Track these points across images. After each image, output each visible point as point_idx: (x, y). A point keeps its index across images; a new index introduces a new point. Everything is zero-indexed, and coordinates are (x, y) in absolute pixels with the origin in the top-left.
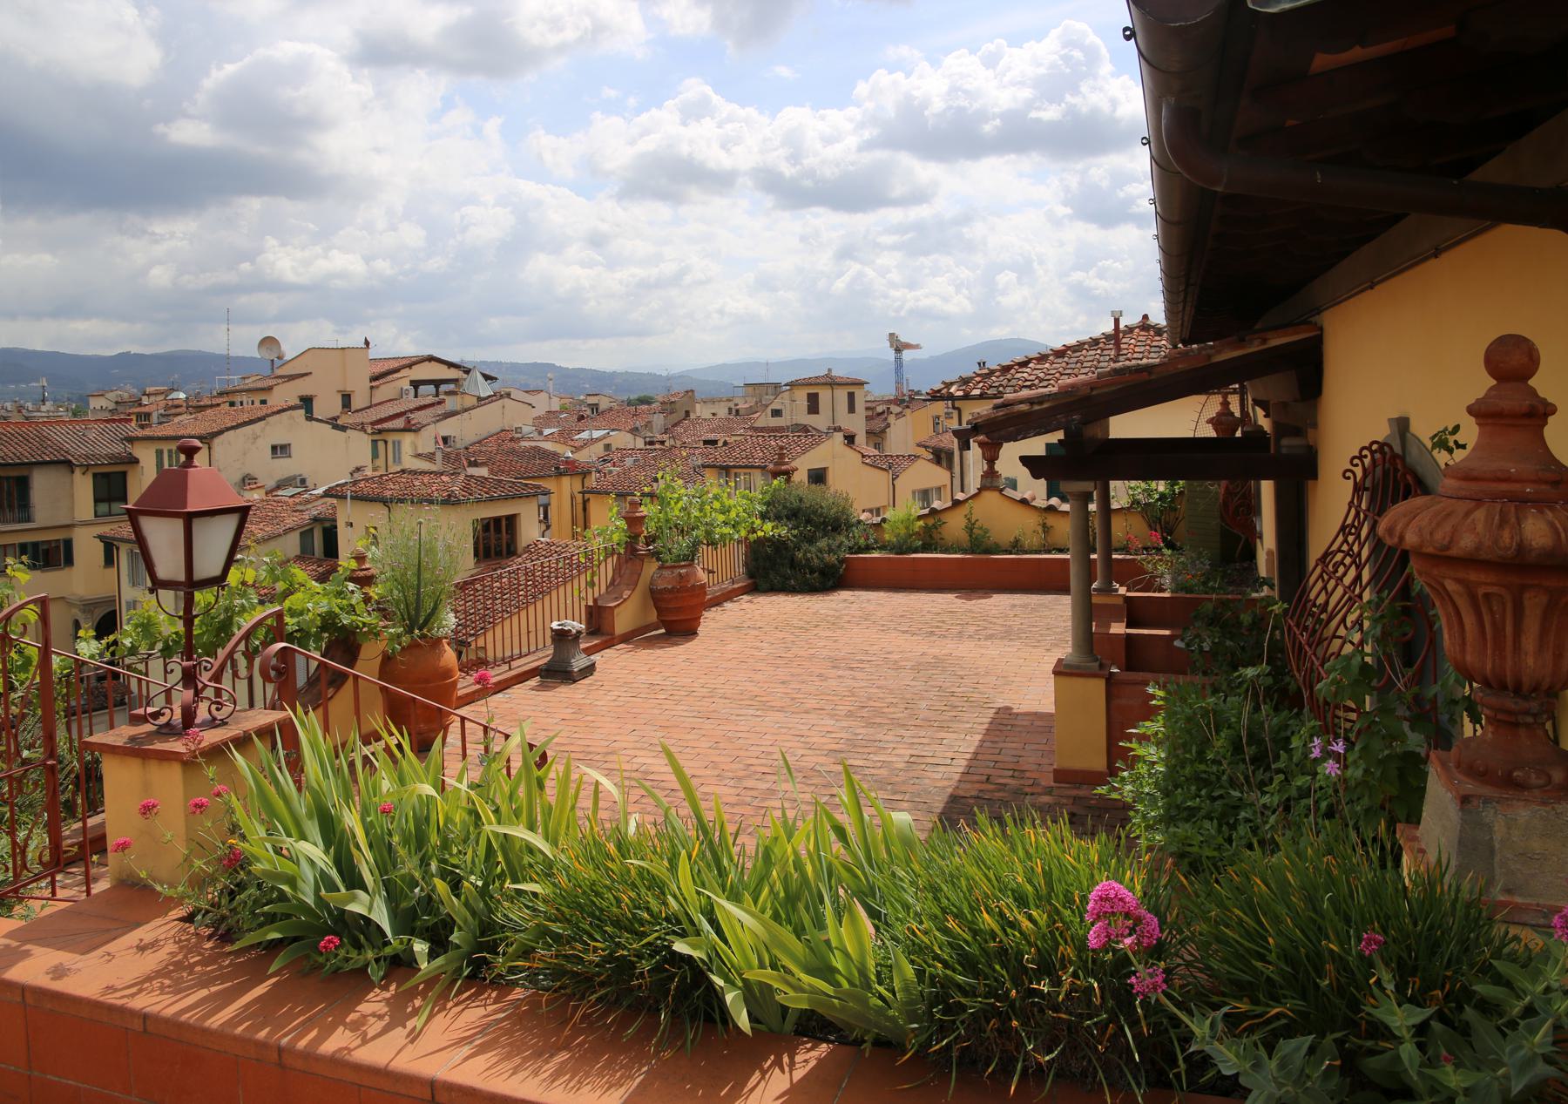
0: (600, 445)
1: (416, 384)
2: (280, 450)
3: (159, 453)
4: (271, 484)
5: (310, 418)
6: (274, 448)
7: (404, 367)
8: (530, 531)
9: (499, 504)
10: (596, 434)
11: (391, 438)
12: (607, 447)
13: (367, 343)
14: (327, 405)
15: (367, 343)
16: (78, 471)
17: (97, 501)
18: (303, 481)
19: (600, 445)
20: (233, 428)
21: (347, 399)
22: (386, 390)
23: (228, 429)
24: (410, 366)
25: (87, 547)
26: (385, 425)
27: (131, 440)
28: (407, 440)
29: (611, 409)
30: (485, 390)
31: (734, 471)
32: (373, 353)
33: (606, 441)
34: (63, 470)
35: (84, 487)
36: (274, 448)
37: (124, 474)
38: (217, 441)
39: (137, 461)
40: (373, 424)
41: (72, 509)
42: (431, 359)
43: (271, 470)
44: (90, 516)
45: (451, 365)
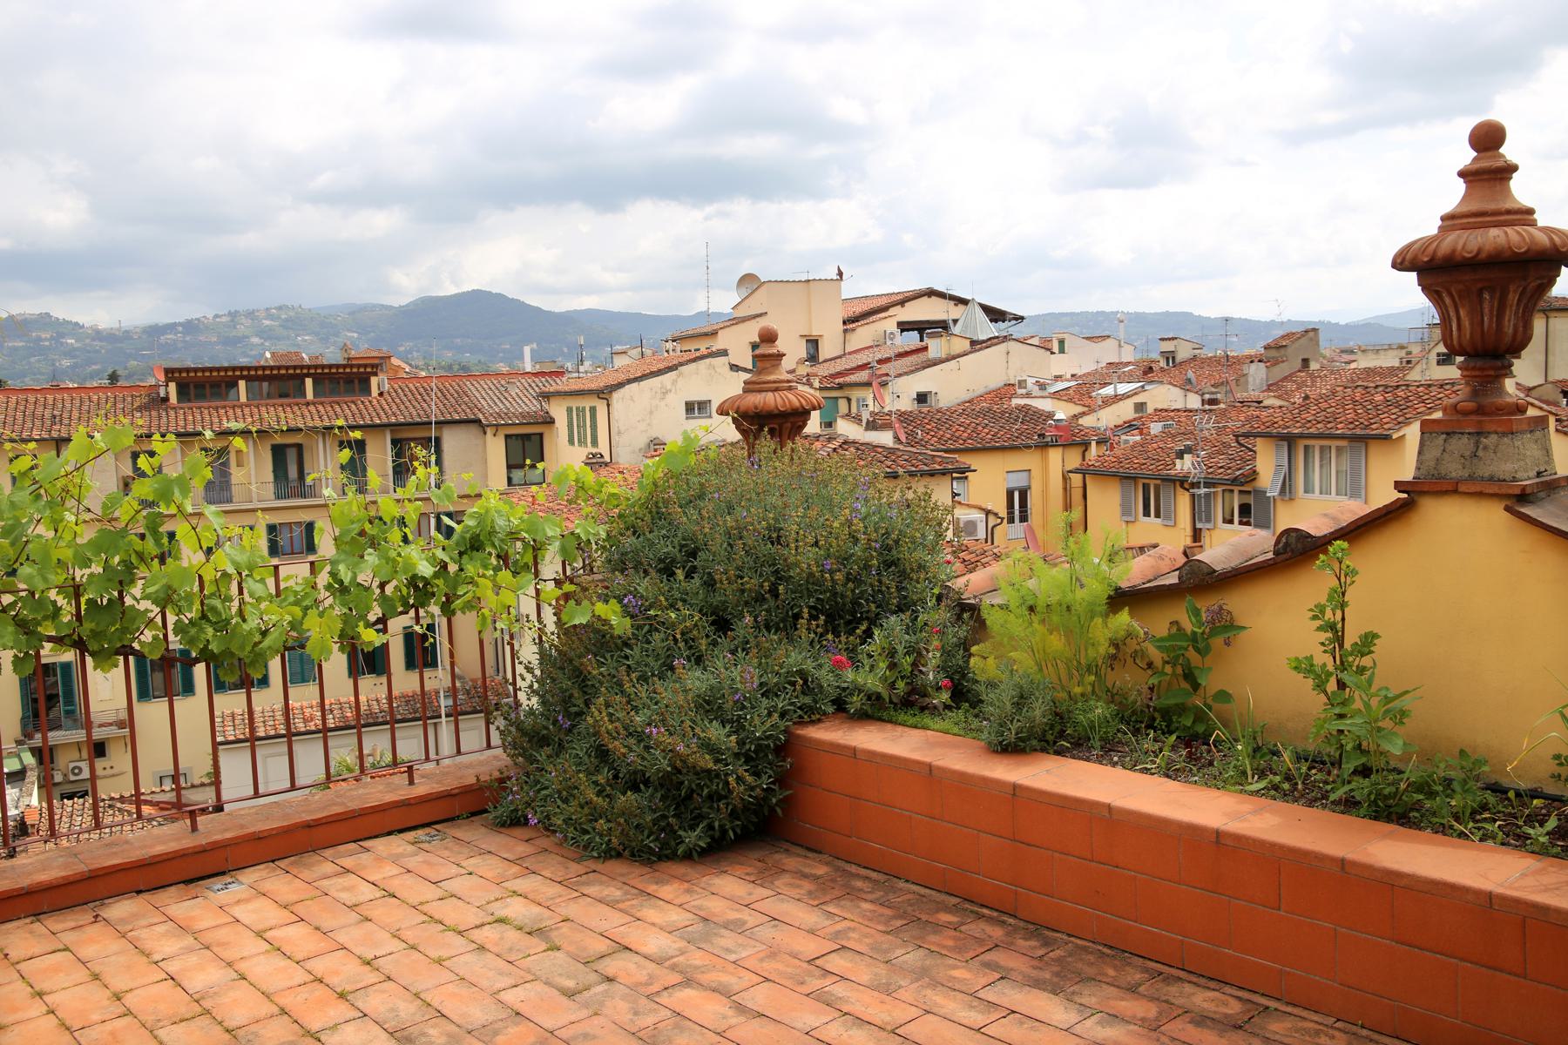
1: (904, 327)
3: (569, 410)
6: (690, 407)
12: (1140, 407)
13: (840, 274)
15: (840, 274)
16: (489, 431)
17: (510, 467)
21: (813, 343)
22: (864, 335)
23: (630, 381)
24: (902, 303)
27: (547, 396)
31: (1301, 444)
32: (849, 289)
34: (474, 429)
35: (496, 449)
37: (541, 435)
38: (617, 396)
39: (552, 422)
42: (931, 293)
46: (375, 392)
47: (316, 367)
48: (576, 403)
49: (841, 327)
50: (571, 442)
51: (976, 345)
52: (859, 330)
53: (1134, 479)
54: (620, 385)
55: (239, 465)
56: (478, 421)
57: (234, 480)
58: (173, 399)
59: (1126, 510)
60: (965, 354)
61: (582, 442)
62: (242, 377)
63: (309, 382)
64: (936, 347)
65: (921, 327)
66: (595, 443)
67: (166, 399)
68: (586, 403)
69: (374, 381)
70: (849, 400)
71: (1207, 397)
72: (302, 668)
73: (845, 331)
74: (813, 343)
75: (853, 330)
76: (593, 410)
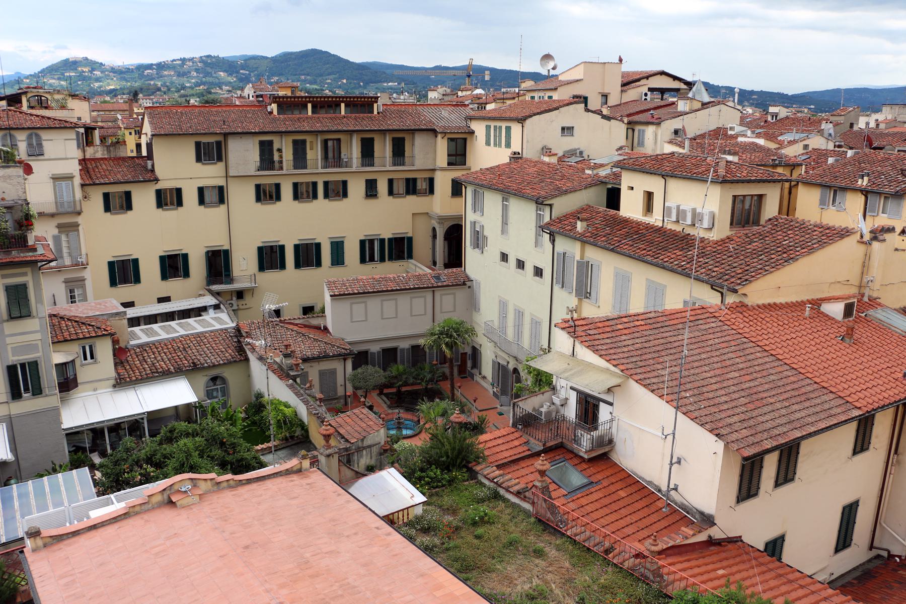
0: (801, 145)
2: (567, 130)
4: (560, 154)
5: (587, 110)
6: (563, 129)
7: (643, 78)
8: (771, 209)
9: (752, 185)
10: (798, 136)
11: (638, 128)
13: (621, 60)
14: (595, 102)
15: (621, 60)
16: (439, 136)
18: (581, 153)
19: (801, 145)
20: (538, 114)
21: (605, 96)
22: (633, 94)
23: (535, 115)
24: (647, 78)
25: (443, 182)
26: (636, 118)
27: (471, 118)
28: (650, 130)
29: (787, 118)
30: (706, 98)
32: (625, 68)
33: (805, 143)
34: (431, 135)
35: (442, 147)
36: (563, 129)
37: (465, 139)
39: (473, 132)
40: (629, 115)
41: (435, 159)
42: (663, 73)
43: (562, 145)
44: (445, 165)
45: (675, 78)
46: (375, 112)
47: (347, 97)
48: (492, 124)
49: (619, 88)
50: (488, 143)
51: (705, 105)
52: (629, 91)
53: (830, 187)
54: (530, 116)
55: (311, 149)
56: (434, 132)
57: (309, 157)
58: (275, 112)
59: (823, 202)
60: (699, 110)
61: (497, 144)
62: (310, 102)
63: (343, 105)
64: (682, 106)
65: (662, 91)
66: (508, 145)
67: (271, 113)
68: (504, 125)
69: (375, 105)
70: (633, 130)
71: (837, 143)
72: (338, 258)
73: (622, 91)
74: (605, 96)
75: (625, 91)
76: (508, 129)
